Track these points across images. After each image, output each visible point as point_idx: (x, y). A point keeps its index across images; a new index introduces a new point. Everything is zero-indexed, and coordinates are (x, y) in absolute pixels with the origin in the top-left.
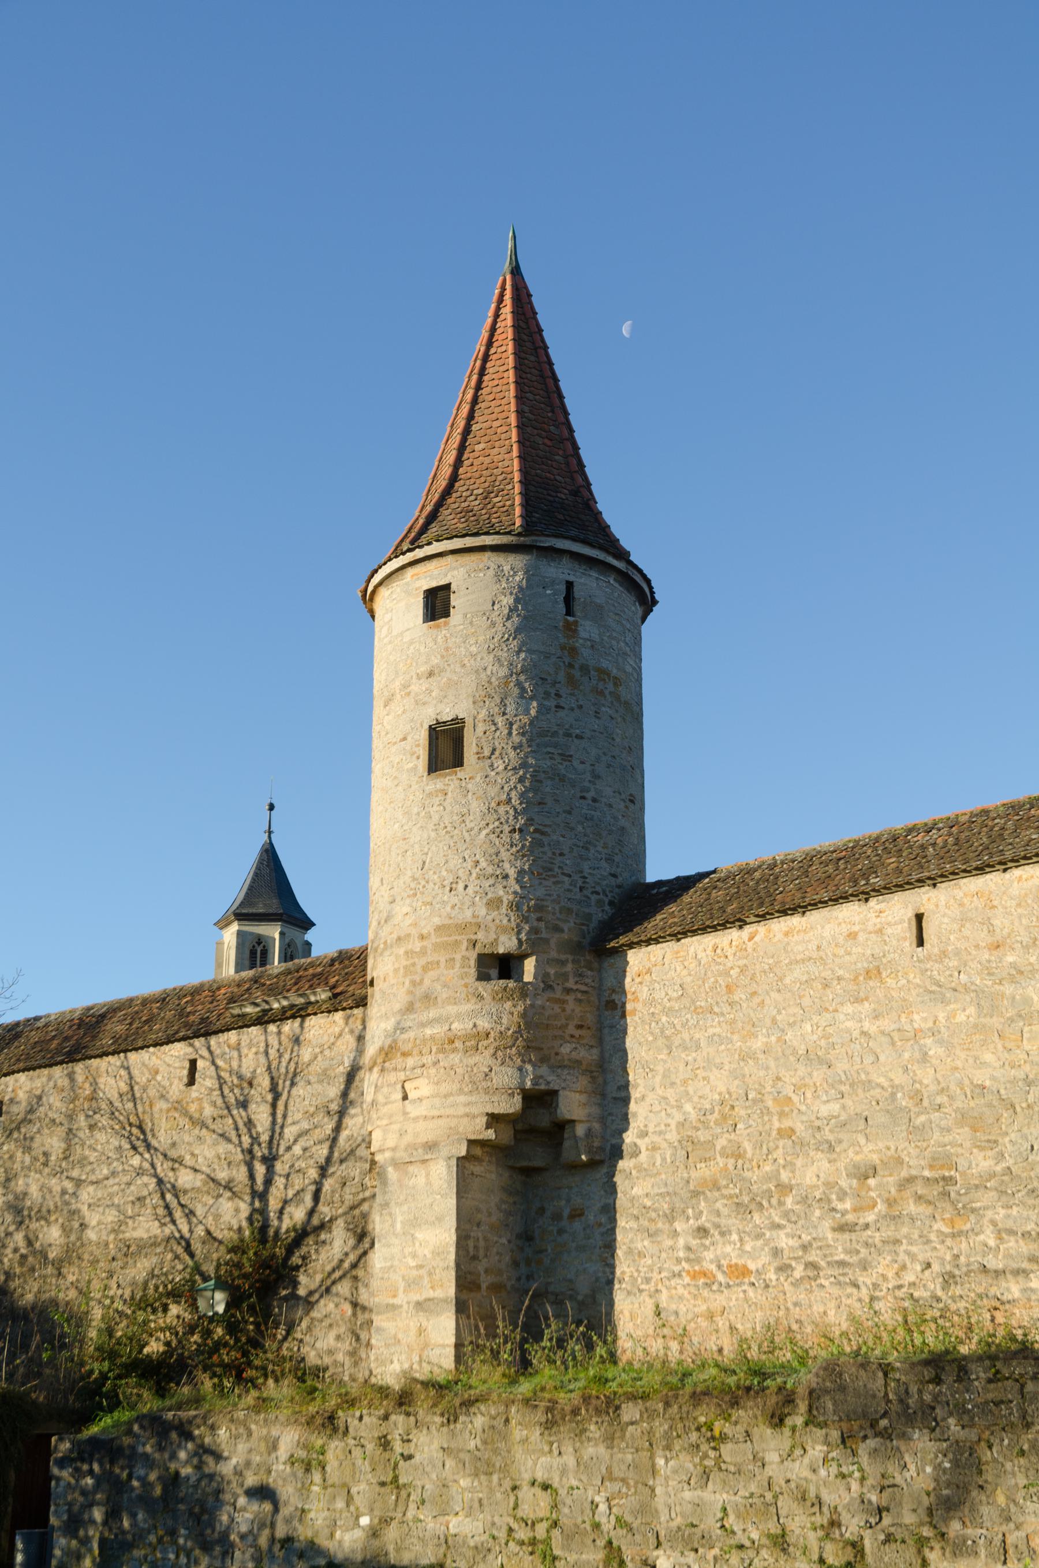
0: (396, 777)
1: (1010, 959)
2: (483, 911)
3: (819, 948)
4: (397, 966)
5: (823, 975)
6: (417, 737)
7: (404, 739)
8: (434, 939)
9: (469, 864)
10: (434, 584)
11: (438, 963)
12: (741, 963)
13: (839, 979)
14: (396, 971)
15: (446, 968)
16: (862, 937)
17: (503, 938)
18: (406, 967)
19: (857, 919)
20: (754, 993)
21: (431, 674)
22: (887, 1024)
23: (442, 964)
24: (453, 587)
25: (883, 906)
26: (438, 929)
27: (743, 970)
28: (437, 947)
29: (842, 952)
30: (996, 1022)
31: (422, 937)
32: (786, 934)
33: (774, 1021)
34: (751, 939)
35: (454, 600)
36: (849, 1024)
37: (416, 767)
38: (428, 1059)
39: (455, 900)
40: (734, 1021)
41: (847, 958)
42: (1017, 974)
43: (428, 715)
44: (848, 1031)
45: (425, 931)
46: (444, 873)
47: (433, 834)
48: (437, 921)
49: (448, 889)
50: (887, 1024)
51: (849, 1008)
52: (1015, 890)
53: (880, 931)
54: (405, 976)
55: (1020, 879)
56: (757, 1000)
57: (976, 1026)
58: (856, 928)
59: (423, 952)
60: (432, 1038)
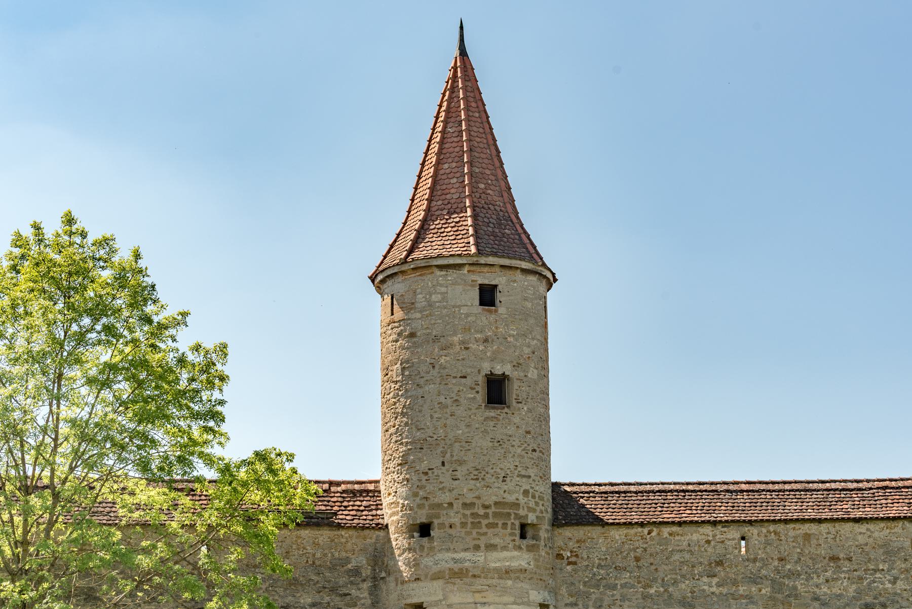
0: (456, 400)
1: (788, 567)
2: (521, 497)
3: (689, 545)
4: (463, 520)
5: (693, 560)
6: (475, 379)
7: (465, 377)
8: (493, 509)
9: (512, 467)
10: (486, 282)
11: (497, 524)
12: (645, 546)
13: (701, 563)
14: (464, 525)
15: (502, 528)
16: (713, 543)
17: (530, 515)
18: (472, 523)
19: (711, 534)
20: (651, 564)
21: (486, 340)
22: (724, 590)
23: (500, 525)
24: (500, 288)
25: (725, 529)
26: (496, 503)
27: (645, 550)
28: (495, 515)
29: (703, 549)
30: (780, 596)
31: (486, 507)
32: (670, 534)
33: (663, 580)
34: (649, 533)
35: (499, 297)
36: (706, 587)
37: (474, 398)
38: (494, 582)
39: (506, 487)
40: (639, 577)
41: (705, 554)
42: (792, 574)
43: (486, 367)
44: (704, 590)
45: (487, 503)
46: (499, 470)
47: (491, 444)
48: (494, 498)
49: (501, 479)
50: (724, 590)
51: (705, 579)
52: (792, 533)
53: (723, 542)
54: (473, 528)
55: (794, 529)
56: (653, 567)
57: (770, 597)
58: (710, 538)
59: (486, 516)
60: (495, 569)
